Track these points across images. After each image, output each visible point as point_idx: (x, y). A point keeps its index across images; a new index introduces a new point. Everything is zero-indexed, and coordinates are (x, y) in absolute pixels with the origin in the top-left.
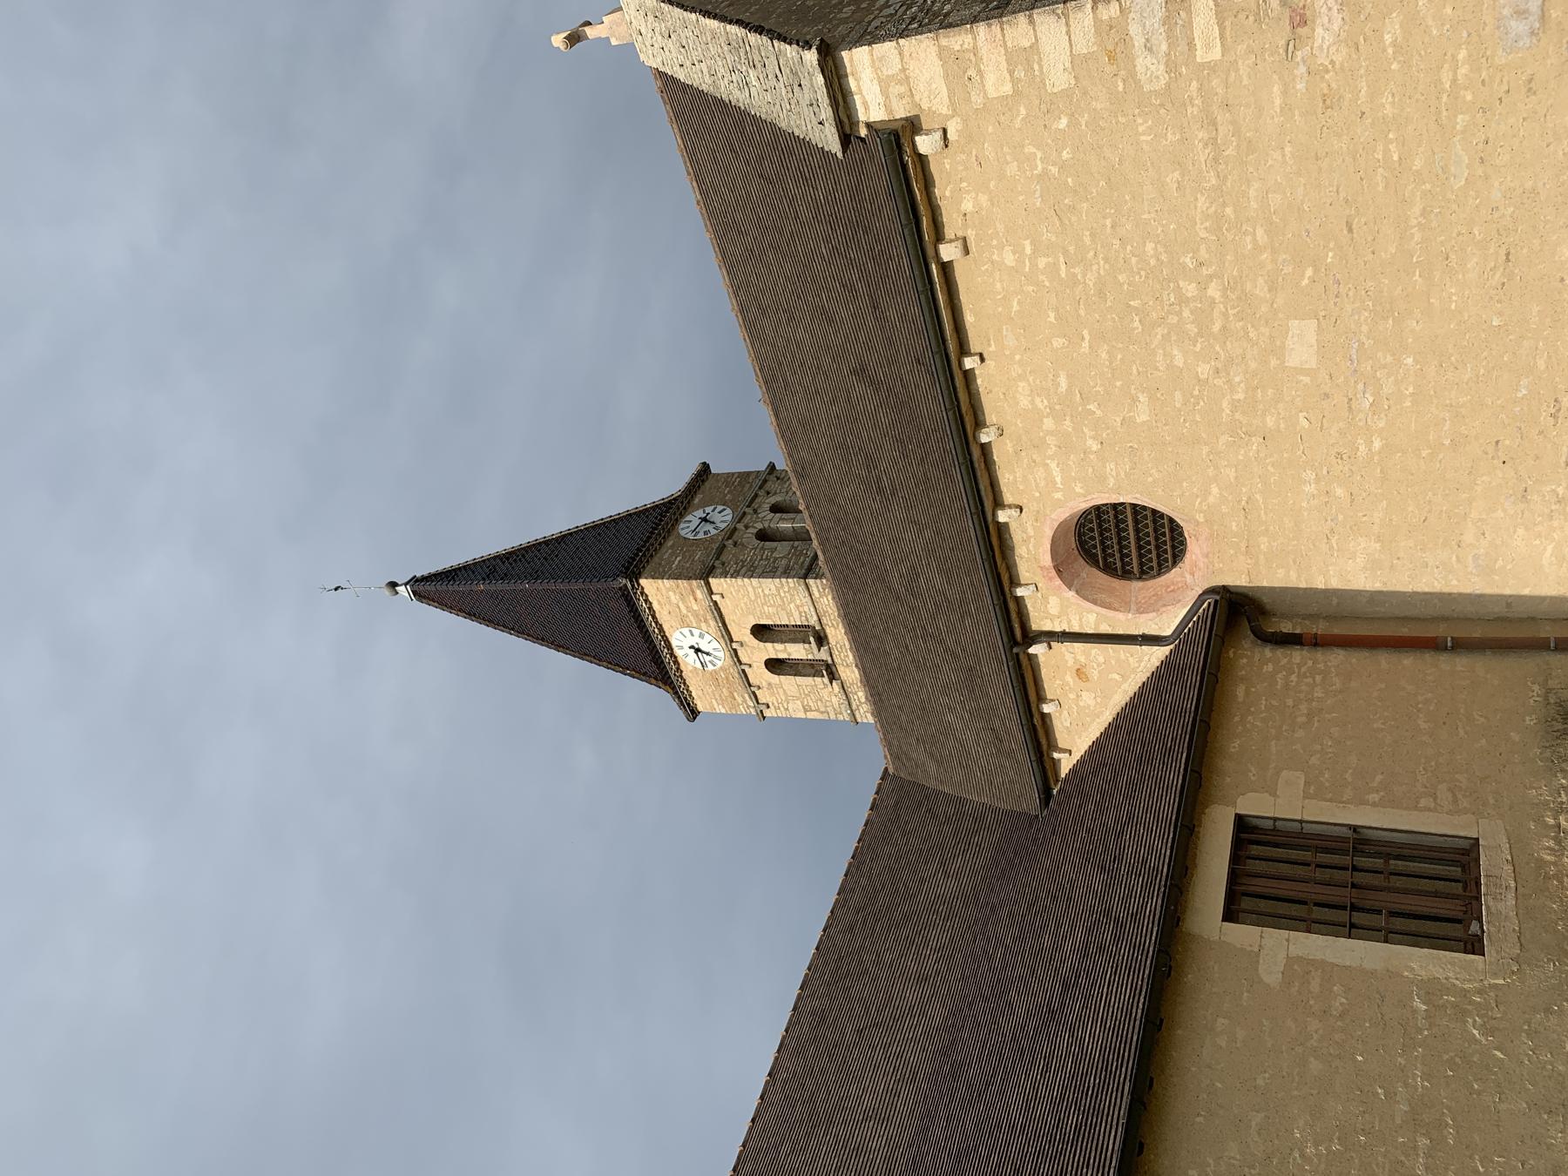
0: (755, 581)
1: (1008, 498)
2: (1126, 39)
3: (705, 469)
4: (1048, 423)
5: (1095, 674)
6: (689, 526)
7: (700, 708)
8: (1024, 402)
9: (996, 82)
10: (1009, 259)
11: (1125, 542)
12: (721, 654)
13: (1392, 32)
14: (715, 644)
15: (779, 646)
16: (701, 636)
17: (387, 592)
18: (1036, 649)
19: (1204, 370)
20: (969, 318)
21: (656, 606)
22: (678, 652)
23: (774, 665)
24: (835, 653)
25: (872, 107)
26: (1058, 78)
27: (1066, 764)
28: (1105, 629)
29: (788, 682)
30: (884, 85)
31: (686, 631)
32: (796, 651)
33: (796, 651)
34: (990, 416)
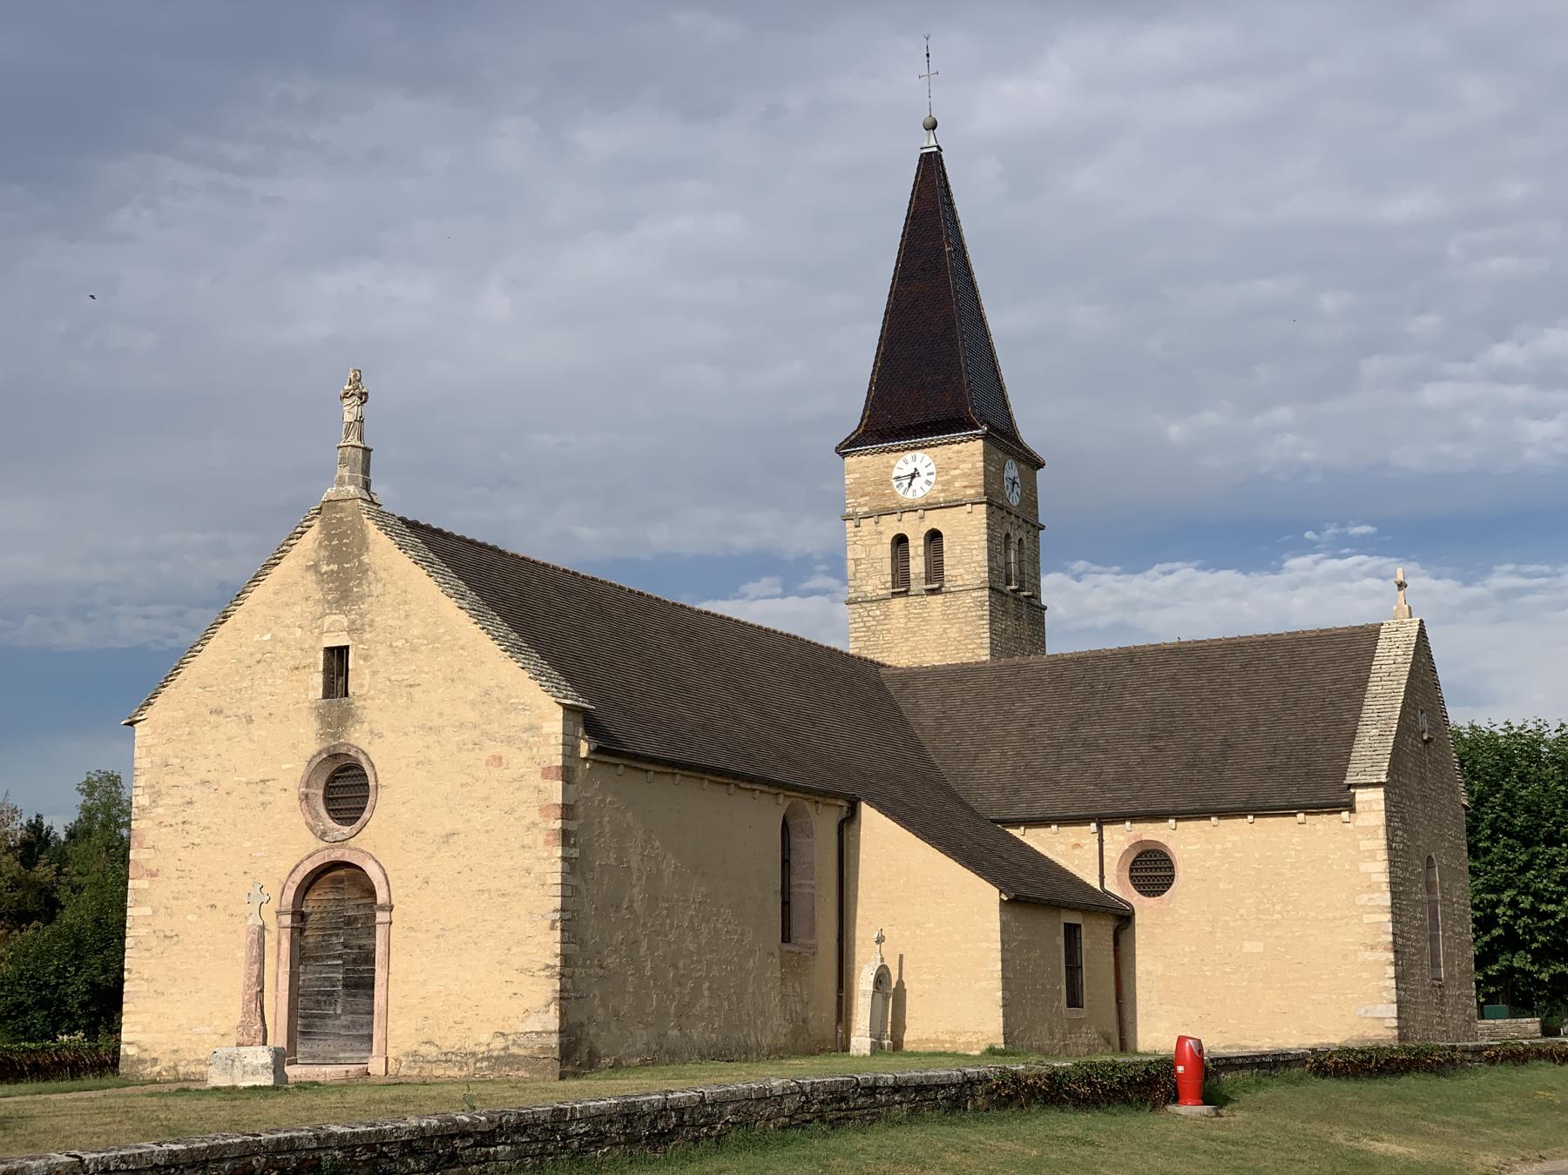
0: (985, 544)
1: (1180, 824)
2: (1374, 891)
3: (1039, 465)
4: (1219, 847)
5: (1077, 852)
6: (1012, 471)
7: (848, 459)
8: (1229, 838)
9: (1365, 845)
10: (1295, 840)
11: (1153, 870)
12: (909, 495)
13: (1365, 975)
14: (920, 494)
15: (921, 550)
16: (928, 482)
17: (924, 116)
18: (1093, 825)
19: (1243, 911)
20: (1270, 820)
21: (955, 447)
22: (909, 455)
23: (901, 540)
24: (919, 599)
25: (1361, 796)
26: (1364, 867)
27: (1016, 833)
28: (1106, 860)
29: (885, 550)
30: (1369, 802)
31: (932, 468)
32: (917, 565)
33: (917, 565)
34: (1223, 822)
